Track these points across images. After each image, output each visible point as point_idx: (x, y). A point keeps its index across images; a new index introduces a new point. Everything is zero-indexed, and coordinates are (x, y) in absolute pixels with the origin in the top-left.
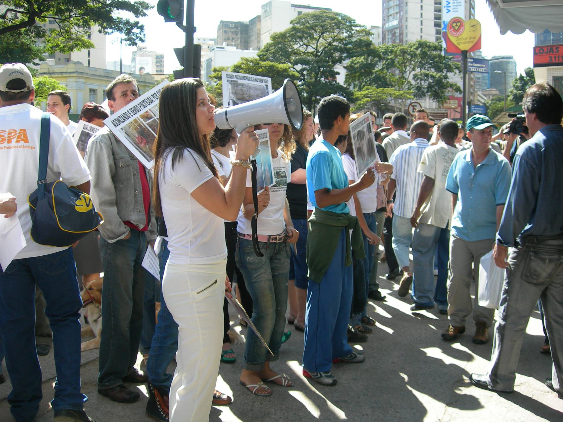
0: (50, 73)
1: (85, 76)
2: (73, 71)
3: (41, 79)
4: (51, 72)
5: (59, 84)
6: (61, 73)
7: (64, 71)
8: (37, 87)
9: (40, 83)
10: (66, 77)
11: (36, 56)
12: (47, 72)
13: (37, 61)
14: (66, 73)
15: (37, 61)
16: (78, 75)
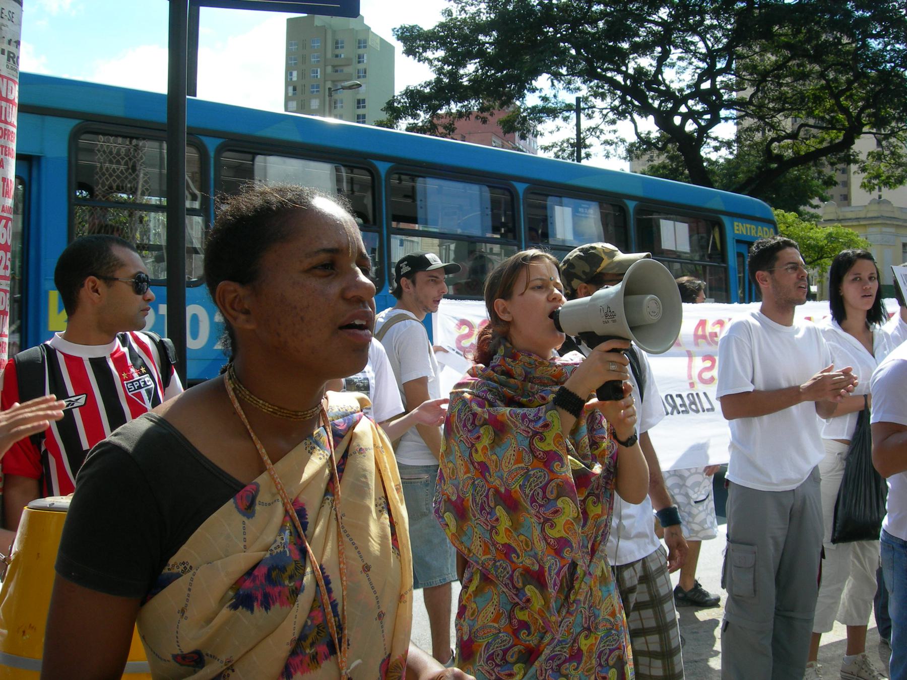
0: (839, 221)
1: (895, 223)
2: (875, 215)
3: (830, 229)
4: (841, 218)
5: (858, 236)
6: (858, 219)
7: (862, 215)
8: (826, 242)
9: (830, 235)
10: (865, 225)
11: (815, 194)
12: (835, 218)
13: (815, 201)
14: (865, 219)
15: (815, 201)
16: (884, 222)
